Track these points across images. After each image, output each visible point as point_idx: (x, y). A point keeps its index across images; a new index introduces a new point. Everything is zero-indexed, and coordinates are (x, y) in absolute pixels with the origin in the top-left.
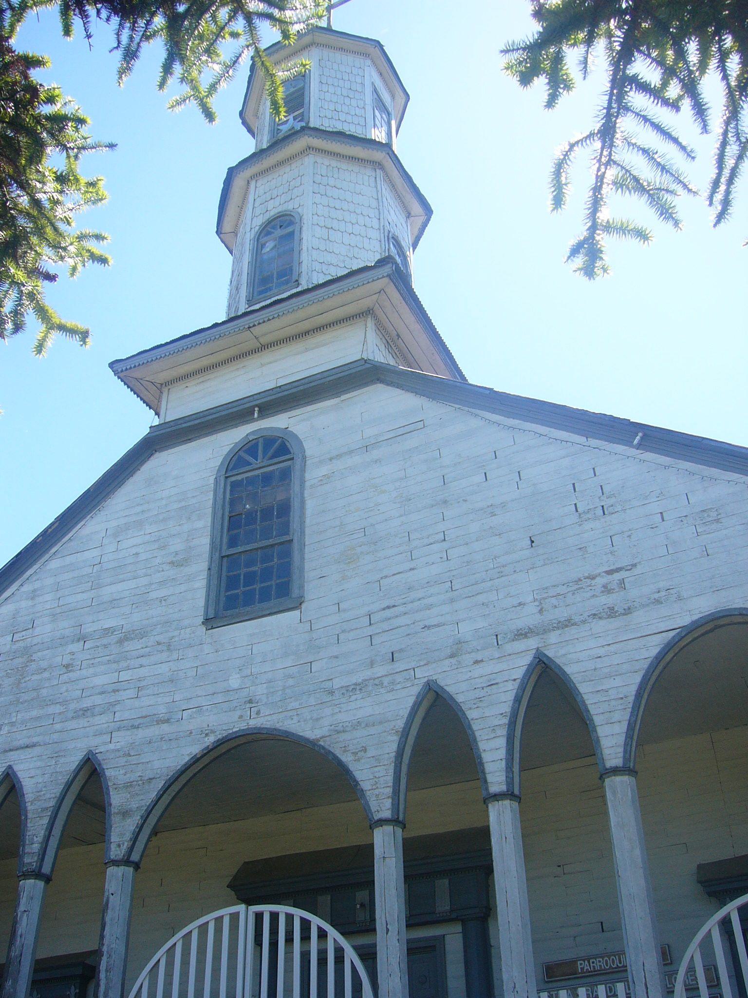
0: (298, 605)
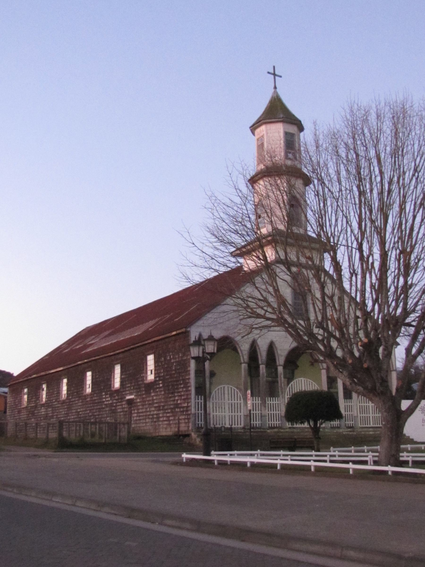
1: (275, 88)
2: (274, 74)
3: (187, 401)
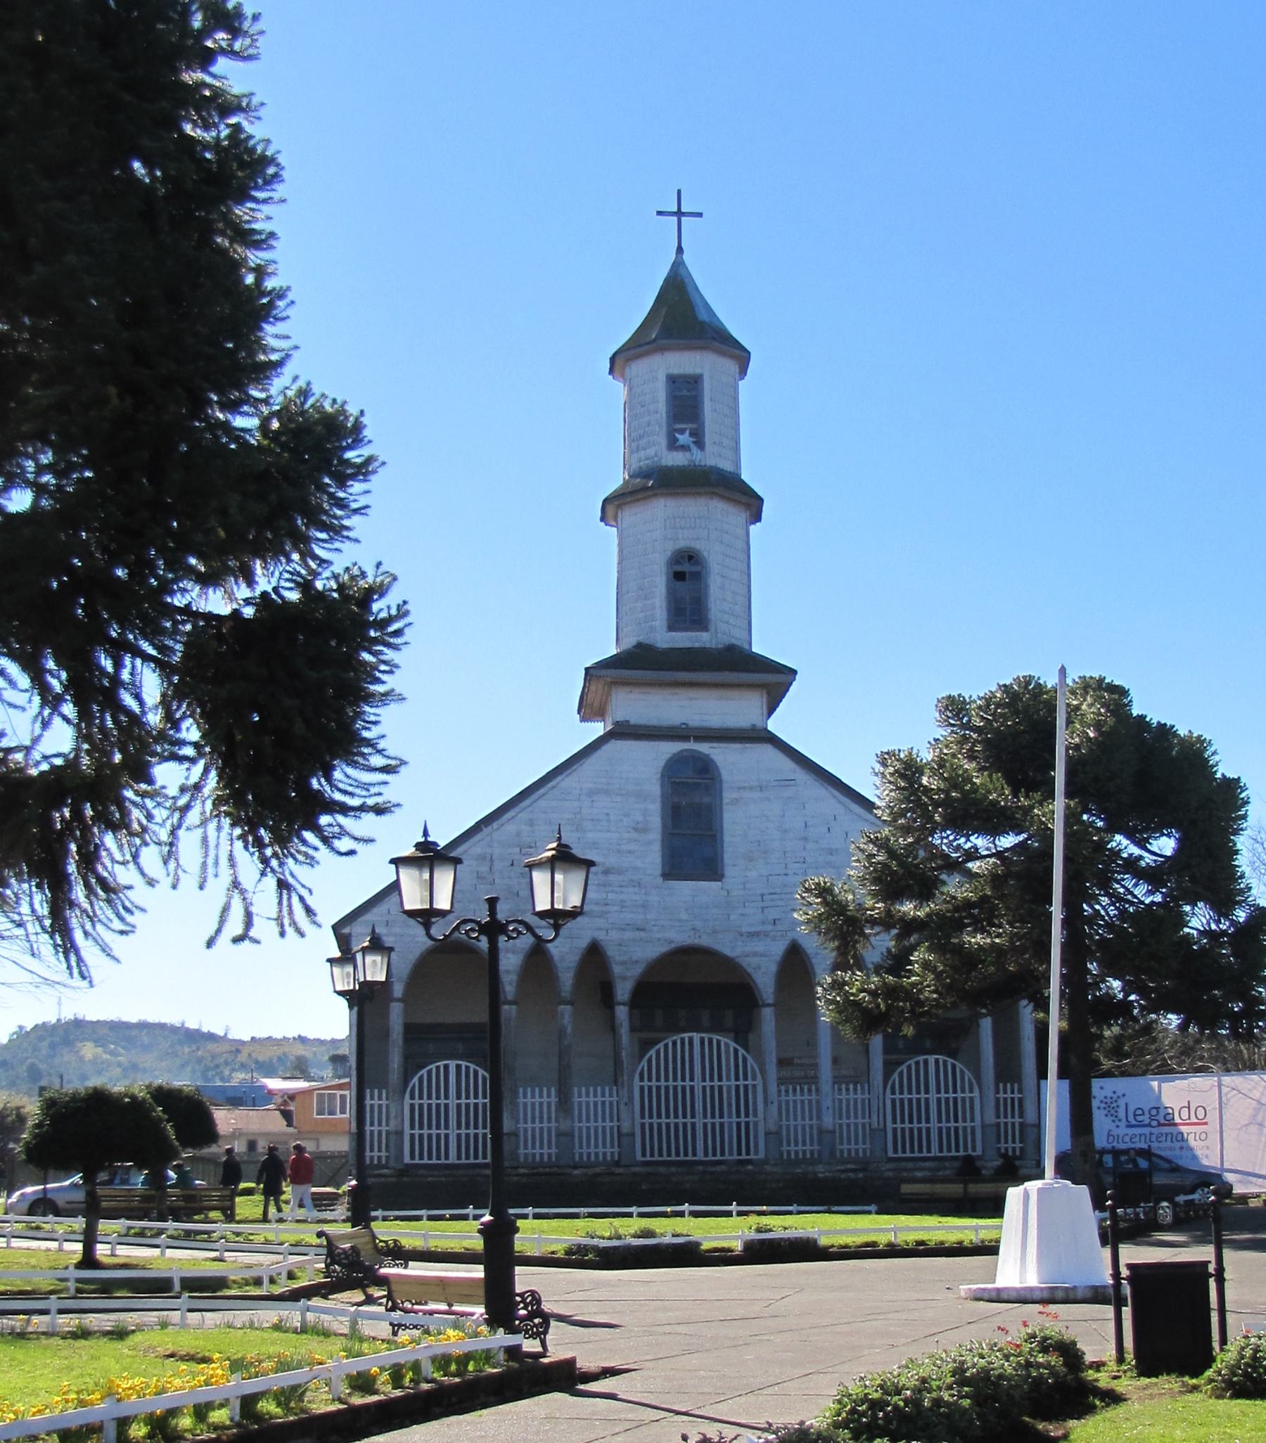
0: (719, 880)
1: (680, 250)
2: (679, 214)
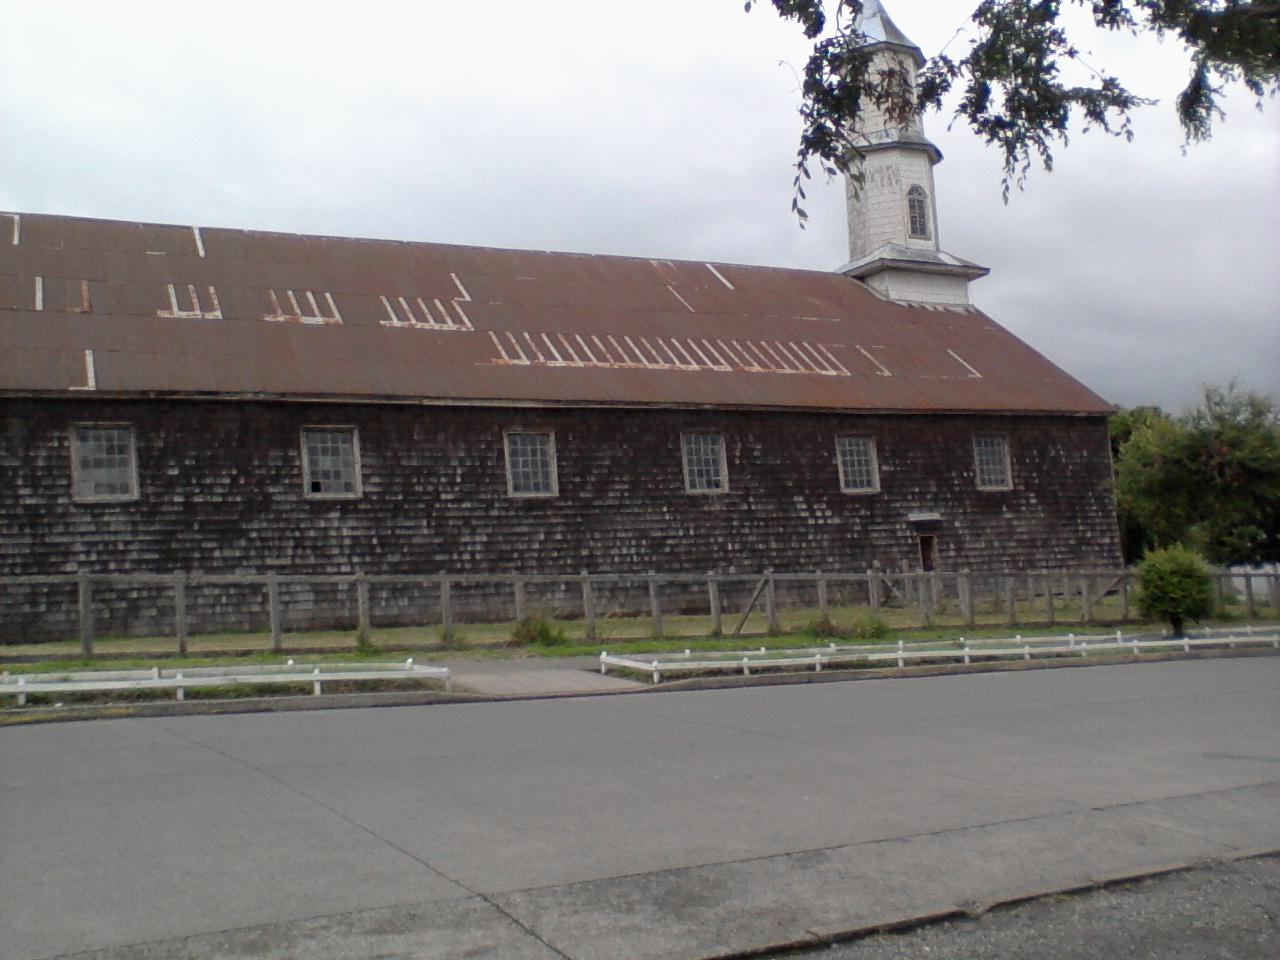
3: (1108, 534)
